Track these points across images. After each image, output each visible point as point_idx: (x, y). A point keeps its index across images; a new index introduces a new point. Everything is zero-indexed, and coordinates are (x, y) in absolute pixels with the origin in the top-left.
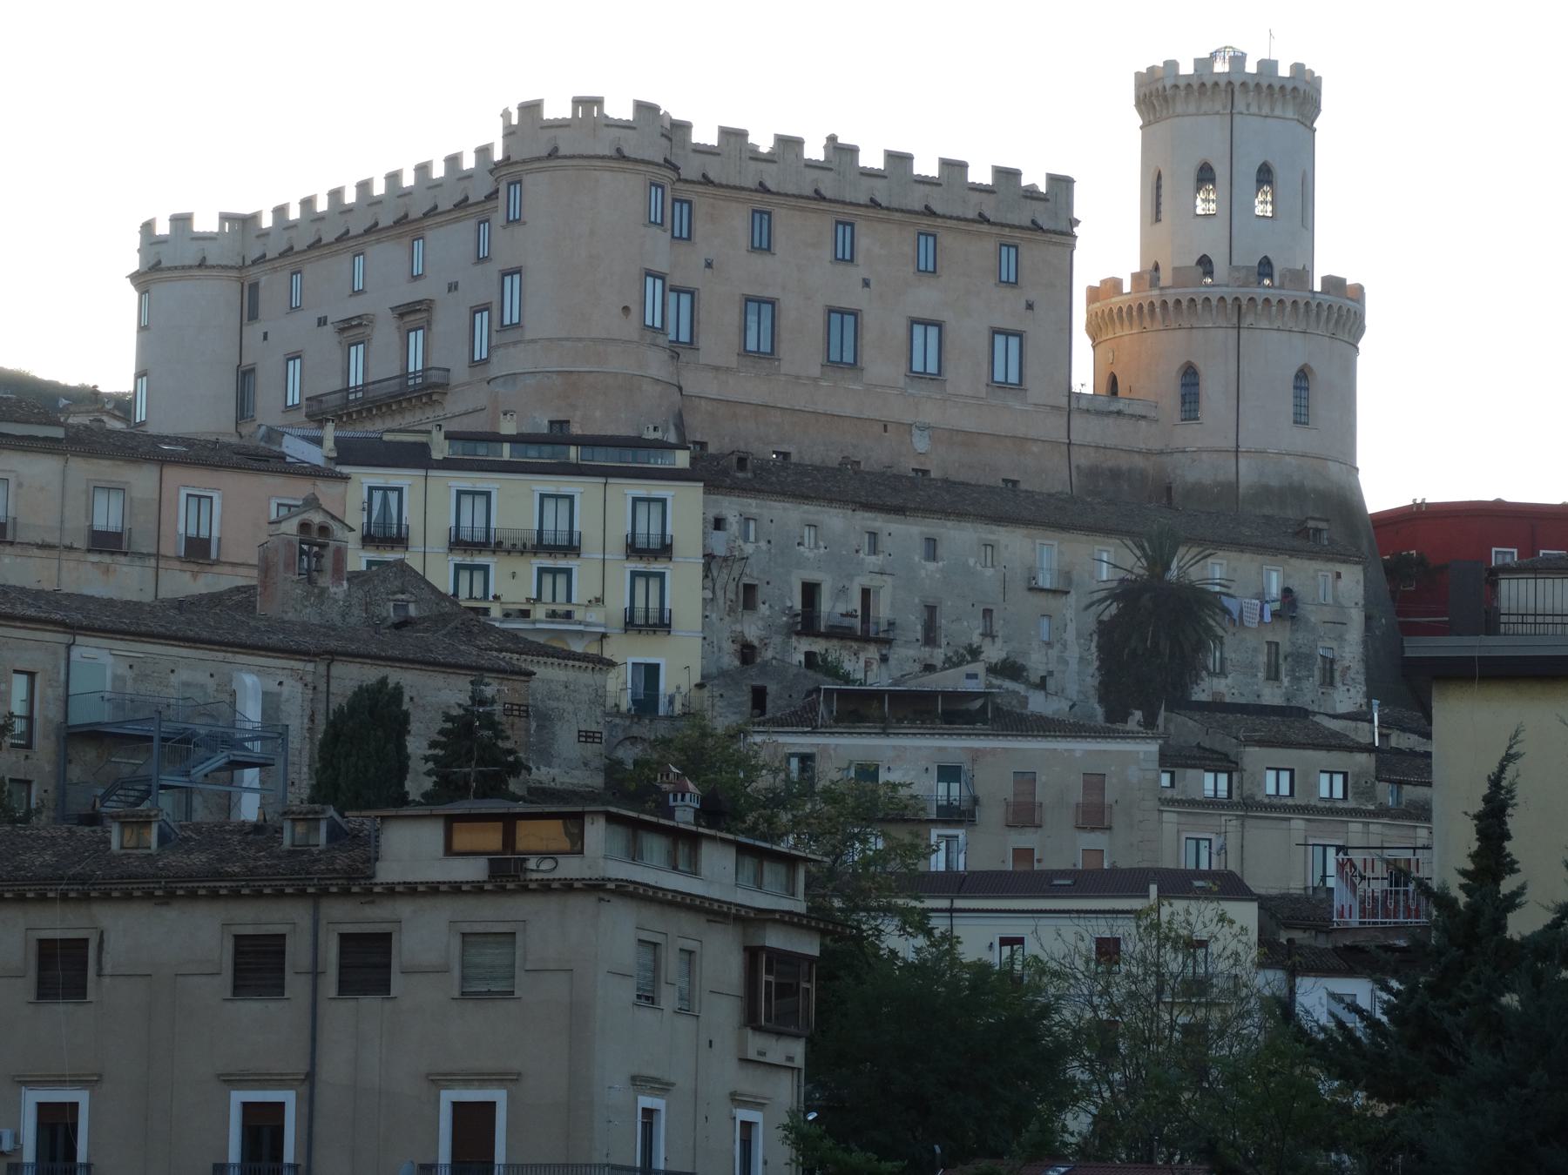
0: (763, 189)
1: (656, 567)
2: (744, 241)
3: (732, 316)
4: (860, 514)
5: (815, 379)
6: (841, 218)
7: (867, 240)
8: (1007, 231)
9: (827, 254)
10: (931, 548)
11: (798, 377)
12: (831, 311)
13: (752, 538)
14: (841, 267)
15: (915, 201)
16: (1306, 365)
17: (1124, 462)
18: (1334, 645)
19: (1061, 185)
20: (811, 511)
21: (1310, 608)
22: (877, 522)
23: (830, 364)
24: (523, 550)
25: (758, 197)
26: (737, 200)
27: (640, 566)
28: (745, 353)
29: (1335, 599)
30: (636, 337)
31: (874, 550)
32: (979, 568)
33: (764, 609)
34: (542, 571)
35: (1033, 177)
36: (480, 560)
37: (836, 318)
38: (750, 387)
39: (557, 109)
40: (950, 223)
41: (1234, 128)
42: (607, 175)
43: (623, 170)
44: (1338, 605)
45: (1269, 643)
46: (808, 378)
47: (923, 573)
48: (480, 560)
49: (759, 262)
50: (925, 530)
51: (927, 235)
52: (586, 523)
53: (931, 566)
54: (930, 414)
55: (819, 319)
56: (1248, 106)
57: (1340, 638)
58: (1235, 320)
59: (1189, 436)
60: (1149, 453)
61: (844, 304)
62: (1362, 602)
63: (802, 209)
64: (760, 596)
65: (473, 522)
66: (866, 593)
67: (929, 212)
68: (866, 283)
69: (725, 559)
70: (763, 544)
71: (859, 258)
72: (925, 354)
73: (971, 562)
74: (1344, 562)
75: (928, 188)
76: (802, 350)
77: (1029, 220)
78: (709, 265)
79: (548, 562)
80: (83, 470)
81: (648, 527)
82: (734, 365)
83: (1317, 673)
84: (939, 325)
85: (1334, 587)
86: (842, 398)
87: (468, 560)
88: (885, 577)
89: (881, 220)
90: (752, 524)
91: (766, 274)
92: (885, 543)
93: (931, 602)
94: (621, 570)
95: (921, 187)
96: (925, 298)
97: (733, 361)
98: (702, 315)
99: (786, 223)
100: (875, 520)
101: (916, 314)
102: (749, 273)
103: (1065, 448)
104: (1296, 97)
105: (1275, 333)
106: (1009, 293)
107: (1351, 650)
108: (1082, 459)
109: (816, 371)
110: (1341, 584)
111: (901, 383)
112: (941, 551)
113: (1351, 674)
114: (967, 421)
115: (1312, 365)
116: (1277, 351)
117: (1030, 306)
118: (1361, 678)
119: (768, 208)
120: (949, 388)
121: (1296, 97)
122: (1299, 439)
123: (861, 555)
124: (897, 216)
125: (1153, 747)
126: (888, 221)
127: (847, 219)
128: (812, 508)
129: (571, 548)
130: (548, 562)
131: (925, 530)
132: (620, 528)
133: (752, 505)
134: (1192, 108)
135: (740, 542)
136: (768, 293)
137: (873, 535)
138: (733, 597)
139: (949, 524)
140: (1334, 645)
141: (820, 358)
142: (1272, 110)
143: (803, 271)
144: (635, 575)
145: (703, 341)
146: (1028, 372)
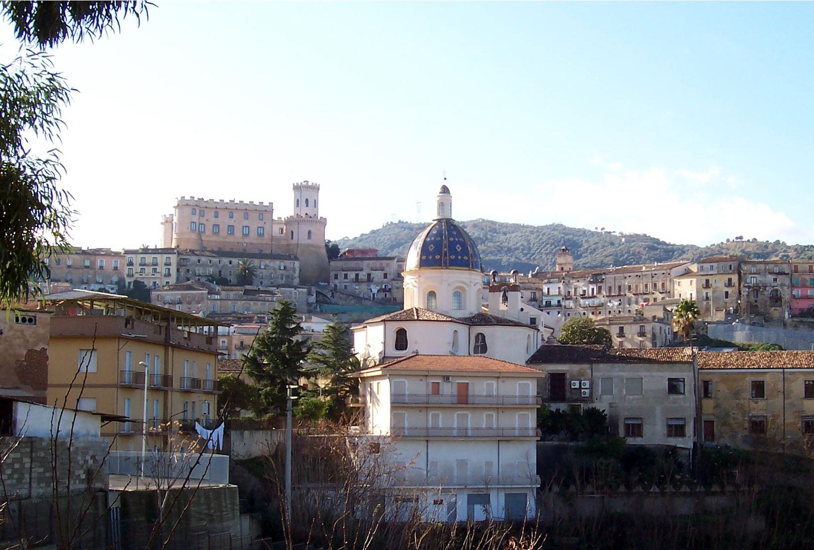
15: (244, 208)
35: (266, 204)
38: (215, 238)
39: (188, 198)
41: (306, 194)
54: (247, 240)
65: (143, 262)
72: (246, 231)
80: (83, 257)
81: (168, 262)
86: (231, 239)
96: (246, 223)
99: (221, 213)
102: (213, 221)
104: (316, 188)
116: (305, 228)
121: (316, 188)
132: (164, 261)
143: (224, 220)
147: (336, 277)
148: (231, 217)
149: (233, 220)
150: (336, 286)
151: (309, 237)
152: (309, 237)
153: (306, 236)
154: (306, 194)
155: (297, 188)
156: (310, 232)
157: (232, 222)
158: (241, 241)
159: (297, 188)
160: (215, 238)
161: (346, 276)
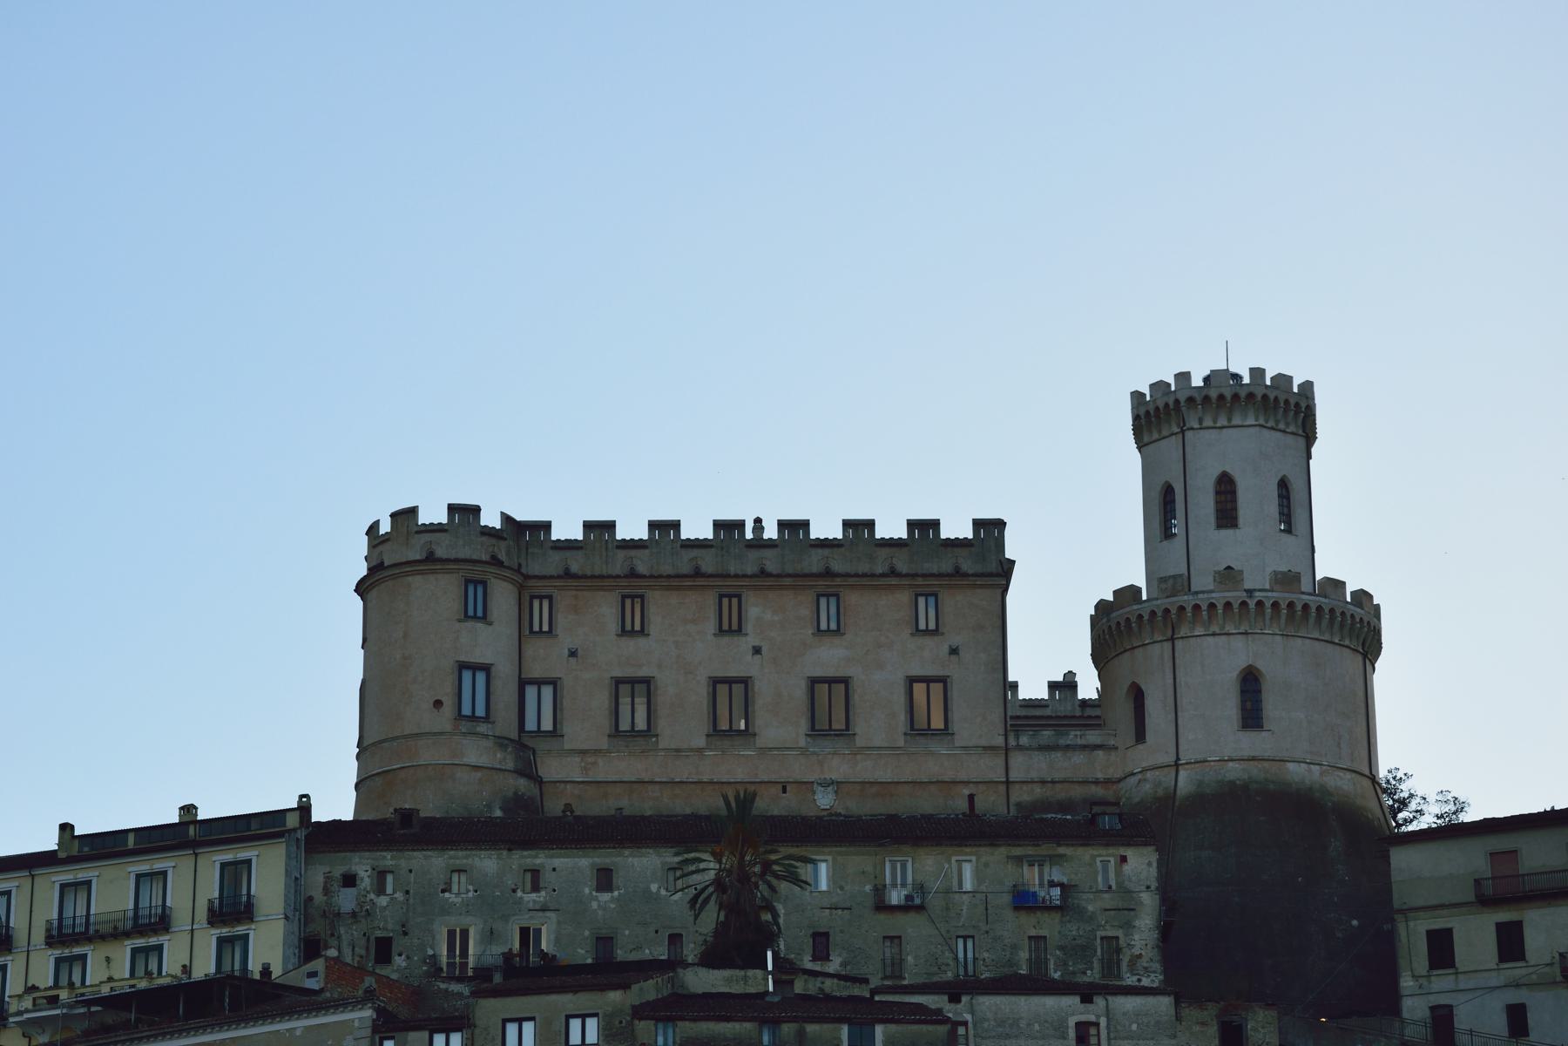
0: (633, 574)
1: (240, 929)
2: (613, 626)
3: (602, 700)
4: (517, 854)
5: (700, 750)
6: (725, 591)
7: (756, 609)
8: (920, 581)
9: (711, 626)
10: (605, 879)
11: (678, 750)
12: (715, 682)
13: (389, 890)
14: (725, 640)
15: (814, 563)
16: (1250, 666)
17: (1077, 792)
18: (1119, 933)
19: (990, 530)
20: (458, 857)
21: (1085, 896)
22: (540, 859)
23: (715, 733)
24: (117, 934)
25: (624, 582)
26: (602, 588)
27: (225, 931)
28: (616, 733)
29: (1120, 884)
30: (448, 727)
31: (536, 888)
32: (663, 892)
33: (399, 961)
34: (135, 951)
35: (956, 527)
36: (77, 950)
37: (722, 690)
38: (624, 766)
40: (851, 581)
42: (419, 578)
43: (434, 572)
44: (1125, 891)
45: (1030, 938)
46: (691, 750)
47: (594, 905)
48: (77, 950)
49: (630, 645)
50: (597, 860)
51: (828, 596)
52: (178, 897)
53: (605, 897)
54: (839, 768)
55: (703, 691)
56: (1201, 421)
57: (1128, 926)
58: (1169, 633)
59: (1141, 757)
60: (1108, 782)
61: (732, 673)
62: (1154, 885)
63: (678, 588)
64: (395, 949)
66: (524, 932)
67: (828, 574)
68: (757, 651)
69: (354, 914)
70: (399, 896)
71: (749, 627)
73: (654, 887)
74: (1129, 845)
75: (826, 552)
76: (683, 725)
77: (964, 571)
78: (573, 654)
79: (140, 942)
82: (605, 746)
83: (1096, 965)
84: (845, 681)
85: (1118, 873)
87: (67, 952)
88: (548, 914)
89: (770, 588)
90: (390, 878)
91: (641, 657)
92: (548, 878)
93: (604, 932)
94: (208, 941)
95: (820, 551)
96: (829, 658)
97: (604, 743)
98: (566, 702)
100: (536, 857)
101: (819, 673)
102: (615, 655)
103: (1002, 788)
105: (1210, 639)
106: (929, 642)
107: (1143, 936)
108: (1021, 795)
109: (701, 742)
110: (1126, 868)
111: (802, 742)
112: (618, 880)
113: (1144, 962)
114: (885, 774)
115: (1260, 665)
117: (954, 651)
118: (1157, 966)
119: (640, 591)
120: (860, 742)
122: (1252, 743)
123: (519, 894)
124: (788, 581)
125: (368, 1013)
126: (781, 588)
127: (731, 591)
128: (460, 853)
129: (163, 923)
130: (140, 942)
131: (597, 860)
133: (388, 859)
134: (1156, 436)
135: (372, 896)
136: (643, 672)
137: (535, 873)
138: (363, 952)
139: (627, 852)
140: (1119, 933)
141: (705, 727)
142: (1230, 420)
144: (222, 942)
145: (567, 729)
146: (956, 715)
147: (1441, 950)
148: (730, 628)
149: (746, 643)
150: (1442, 1018)
151: (1252, 717)
152: (1252, 717)
153: (1230, 708)
154: (1224, 445)
155: (1161, 416)
156: (1250, 682)
157: (736, 658)
158: (798, 770)
159: (1161, 416)
160: (624, 766)
161: (1510, 943)
